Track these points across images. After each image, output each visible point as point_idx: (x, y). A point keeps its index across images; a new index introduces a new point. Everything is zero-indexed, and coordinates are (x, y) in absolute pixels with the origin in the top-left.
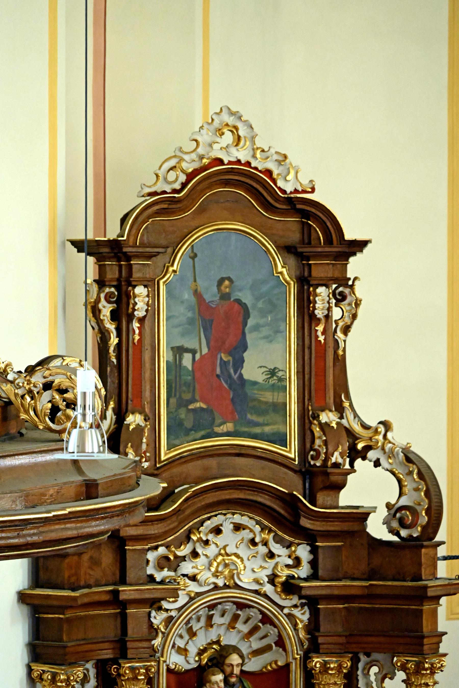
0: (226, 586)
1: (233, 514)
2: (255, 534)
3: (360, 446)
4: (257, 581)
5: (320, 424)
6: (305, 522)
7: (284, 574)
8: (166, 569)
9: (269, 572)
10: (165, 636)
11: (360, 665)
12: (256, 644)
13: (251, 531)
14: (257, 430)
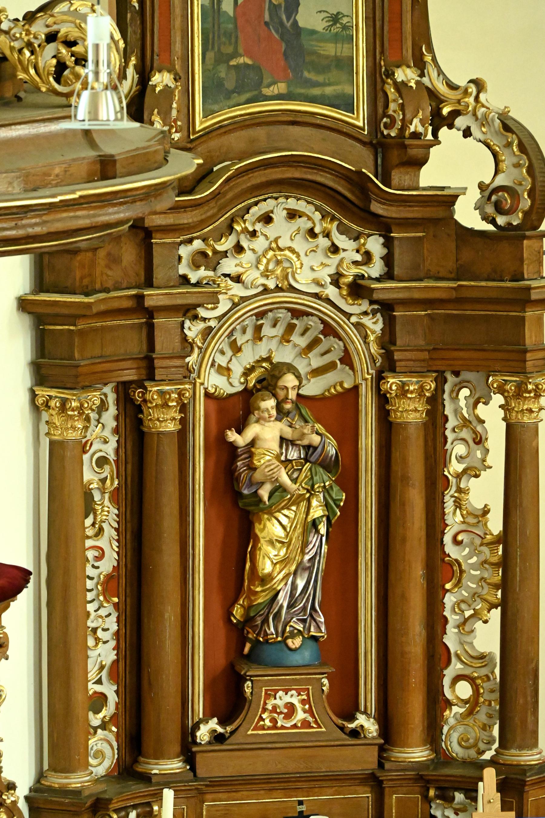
0: (278, 289)
1: (287, 198)
2: (314, 223)
3: (446, 111)
4: (317, 283)
5: (395, 83)
6: (376, 208)
7: (351, 272)
8: (203, 268)
9: (332, 270)
10: (203, 352)
11: (447, 387)
12: (316, 362)
13: (309, 218)
14: (316, 91)
